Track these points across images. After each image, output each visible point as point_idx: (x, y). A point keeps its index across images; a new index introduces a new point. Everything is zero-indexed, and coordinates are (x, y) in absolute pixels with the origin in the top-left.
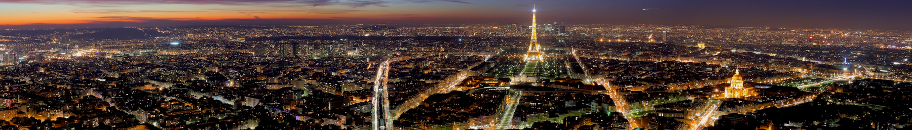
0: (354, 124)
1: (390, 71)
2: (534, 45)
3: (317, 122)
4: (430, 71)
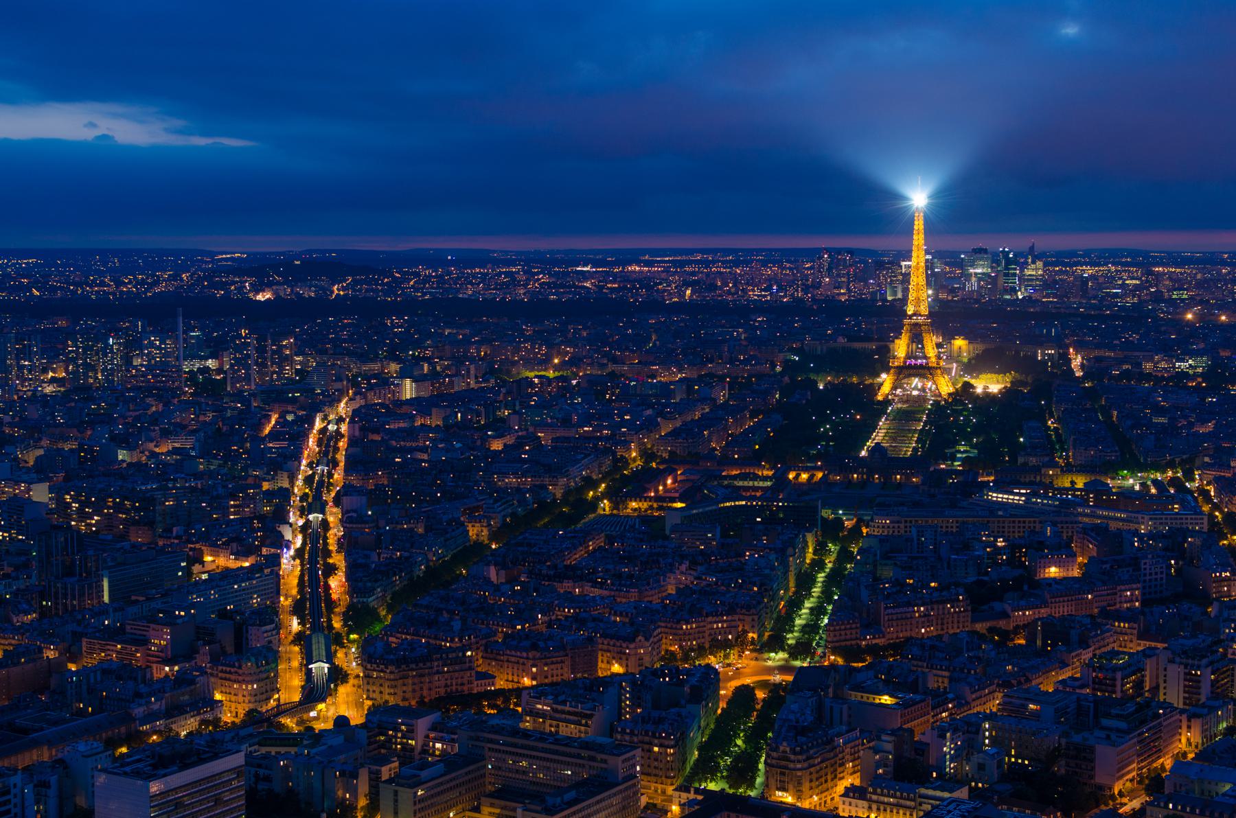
0: (203, 661)
1: (352, 442)
2: (917, 338)
4: (510, 440)
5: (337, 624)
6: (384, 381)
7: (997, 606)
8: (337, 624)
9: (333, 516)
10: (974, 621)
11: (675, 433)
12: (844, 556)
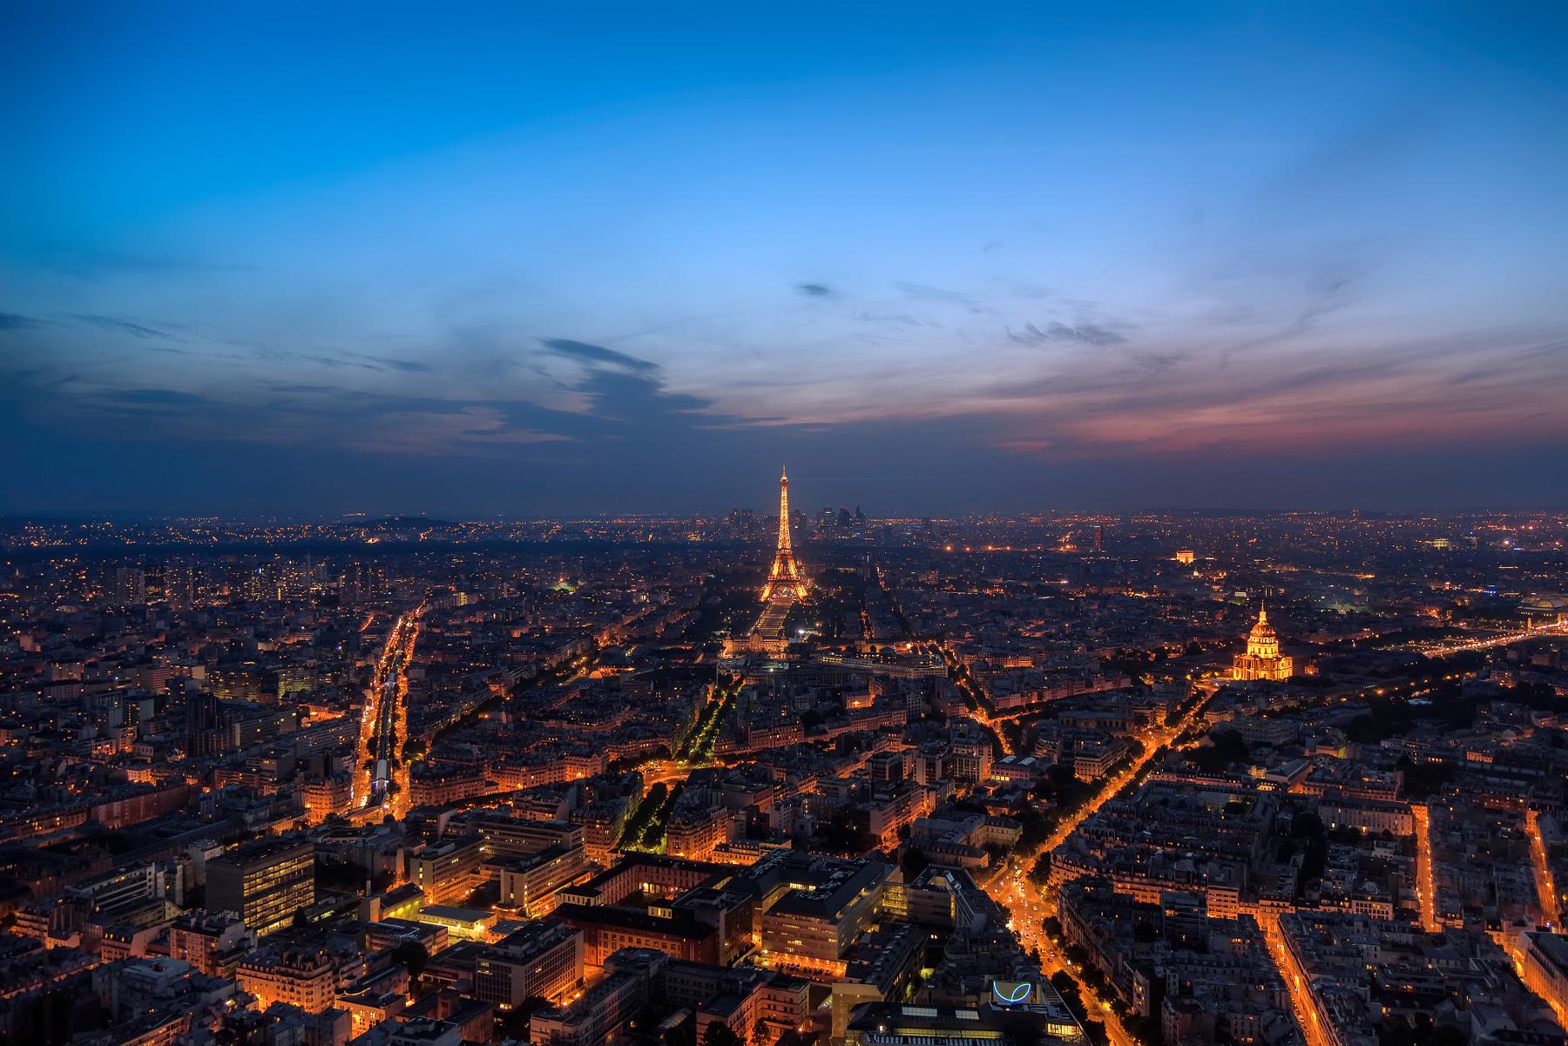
3: (191, 782)
4: (525, 631)
5: (398, 755)
6: (444, 593)
7: (821, 726)
8: (398, 755)
9: (403, 683)
10: (806, 735)
11: (631, 625)
12: (731, 698)
